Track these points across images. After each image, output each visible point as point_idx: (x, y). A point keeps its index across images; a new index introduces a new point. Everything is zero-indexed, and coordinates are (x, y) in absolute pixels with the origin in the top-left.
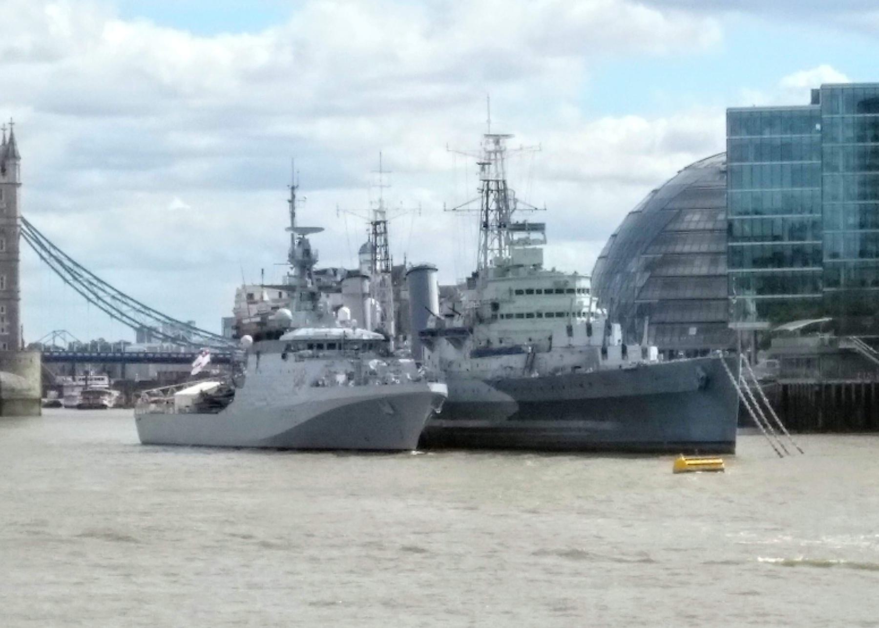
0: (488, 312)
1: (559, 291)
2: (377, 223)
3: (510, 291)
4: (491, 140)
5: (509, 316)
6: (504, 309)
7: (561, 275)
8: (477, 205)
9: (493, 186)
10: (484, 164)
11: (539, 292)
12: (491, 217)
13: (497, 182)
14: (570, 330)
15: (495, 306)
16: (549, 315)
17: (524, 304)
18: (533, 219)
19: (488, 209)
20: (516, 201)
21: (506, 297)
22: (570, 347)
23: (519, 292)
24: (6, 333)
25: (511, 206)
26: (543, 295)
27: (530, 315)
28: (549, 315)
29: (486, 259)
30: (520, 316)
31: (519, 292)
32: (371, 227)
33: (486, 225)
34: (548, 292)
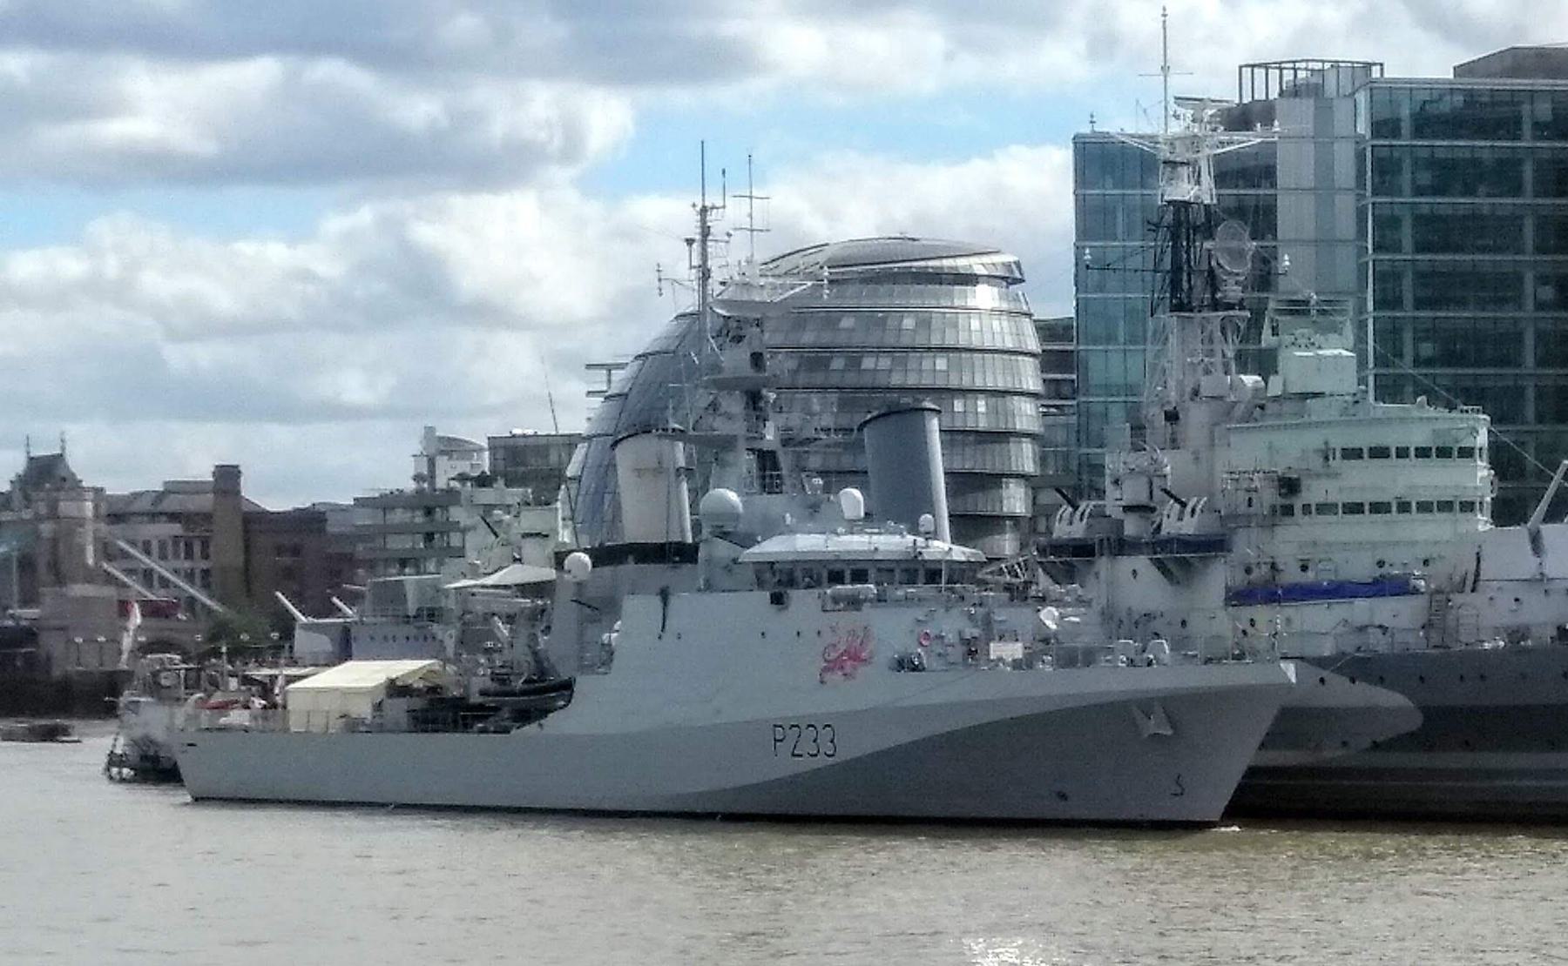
1: (1444, 453)
5: (1324, 508)
6: (1314, 492)
11: (1402, 453)
15: (1290, 486)
16: (1425, 507)
17: (1364, 480)
21: (1316, 463)
23: (1352, 454)
27: (1379, 508)
28: (1425, 507)
30: (1354, 508)
31: (1352, 454)
34: (1423, 453)
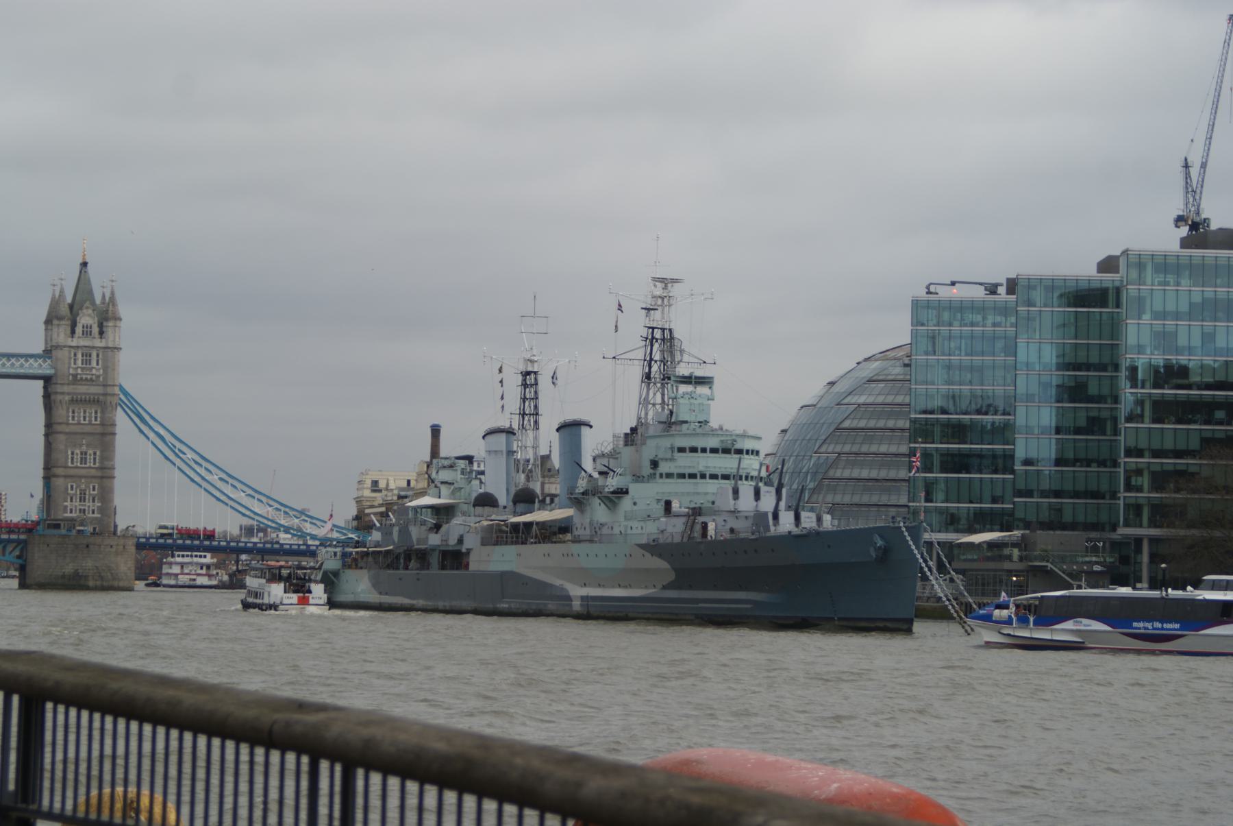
0: (647, 470)
1: (726, 451)
2: (528, 373)
3: (672, 448)
4: (659, 284)
5: (669, 475)
6: (664, 468)
7: (728, 433)
8: (640, 354)
9: (658, 334)
10: (648, 309)
11: (704, 450)
12: (655, 368)
13: (663, 330)
14: (736, 492)
15: (655, 464)
16: (714, 477)
17: (686, 462)
18: (699, 372)
19: (651, 359)
20: (682, 351)
22: (734, 512)
23: (681, 450)
24: (96, 515)
25: (678, 358)
26: (708, 454)
27: (693, 476)
28: (714, 477)
29: (646, 414)
30: (682, 476)
31: (681, 450)
32: (520, 378)
33: (648, 376)
34: (714, 451)
